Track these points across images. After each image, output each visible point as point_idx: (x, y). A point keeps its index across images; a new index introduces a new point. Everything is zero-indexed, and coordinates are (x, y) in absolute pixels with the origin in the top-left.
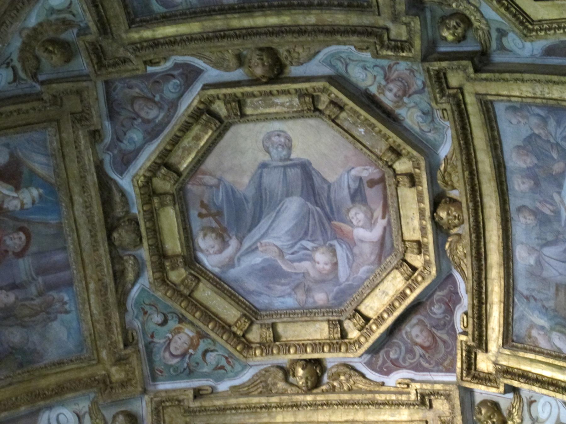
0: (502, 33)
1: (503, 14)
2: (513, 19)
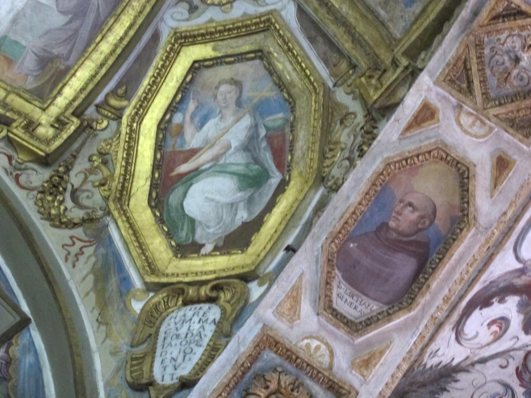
0: (193, 9)
1: (201, 29)
2: (192, 33)
